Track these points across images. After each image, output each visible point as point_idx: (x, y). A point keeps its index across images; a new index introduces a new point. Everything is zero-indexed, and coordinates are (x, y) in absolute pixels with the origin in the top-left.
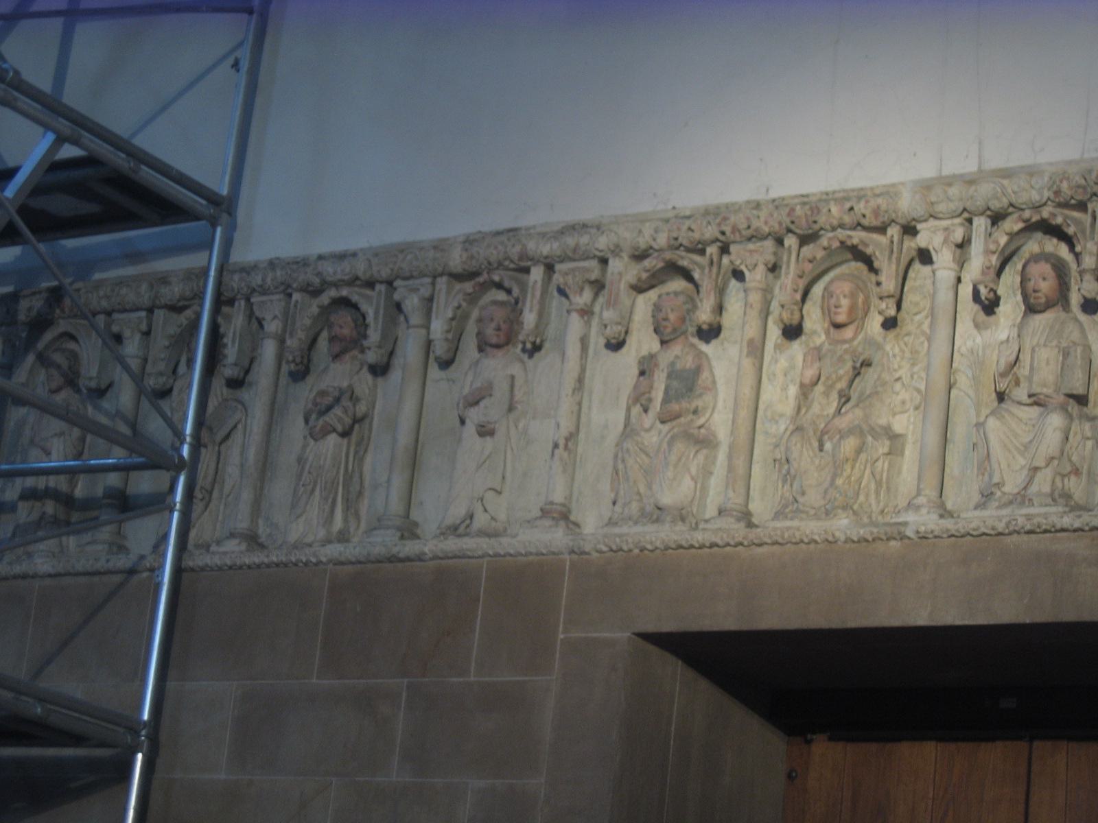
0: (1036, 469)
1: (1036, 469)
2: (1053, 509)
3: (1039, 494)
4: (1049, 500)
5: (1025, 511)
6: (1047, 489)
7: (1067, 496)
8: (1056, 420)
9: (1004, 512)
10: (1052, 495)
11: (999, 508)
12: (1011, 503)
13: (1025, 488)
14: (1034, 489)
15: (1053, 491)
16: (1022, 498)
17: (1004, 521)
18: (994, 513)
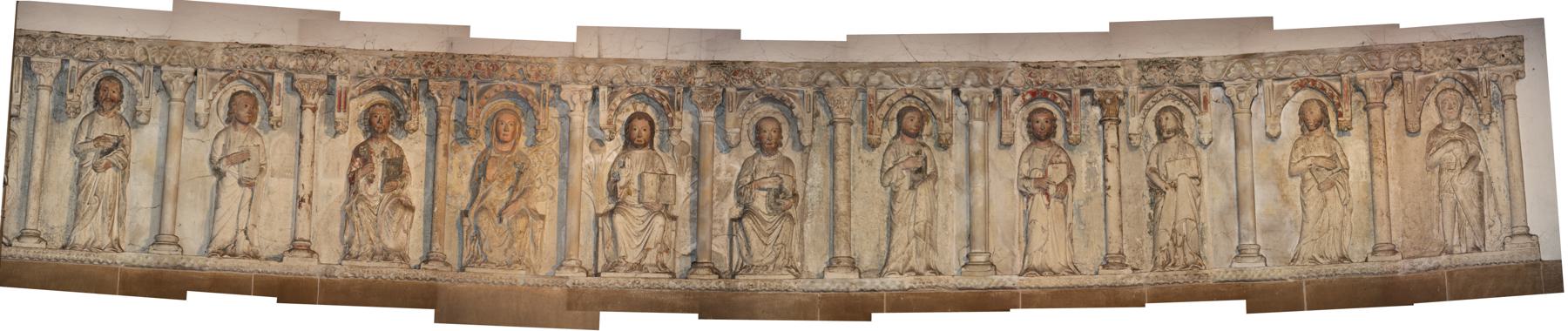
0: (648, 249)
1: (648, 249)
2: (662, 275)
3: (651, 265)
4: (656, 269)
5: (644, 275)
6: (654, 262)
7: (664, 266)
8: (659, 220)
9: (630, 275)
10: (657, 266)
11: (626, 272)
12: (632, 269)
13: (640, 261)
14: (647, 261)
15: (657, 262)
16: (639, 267)
17: (632, 280)
18: (624, 275)
